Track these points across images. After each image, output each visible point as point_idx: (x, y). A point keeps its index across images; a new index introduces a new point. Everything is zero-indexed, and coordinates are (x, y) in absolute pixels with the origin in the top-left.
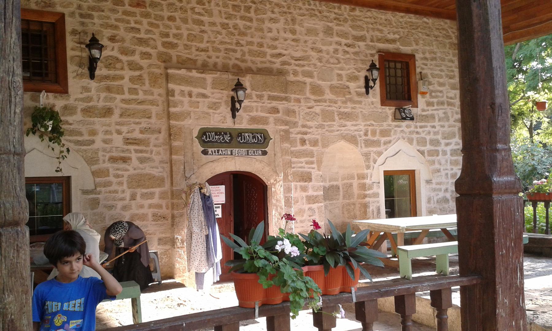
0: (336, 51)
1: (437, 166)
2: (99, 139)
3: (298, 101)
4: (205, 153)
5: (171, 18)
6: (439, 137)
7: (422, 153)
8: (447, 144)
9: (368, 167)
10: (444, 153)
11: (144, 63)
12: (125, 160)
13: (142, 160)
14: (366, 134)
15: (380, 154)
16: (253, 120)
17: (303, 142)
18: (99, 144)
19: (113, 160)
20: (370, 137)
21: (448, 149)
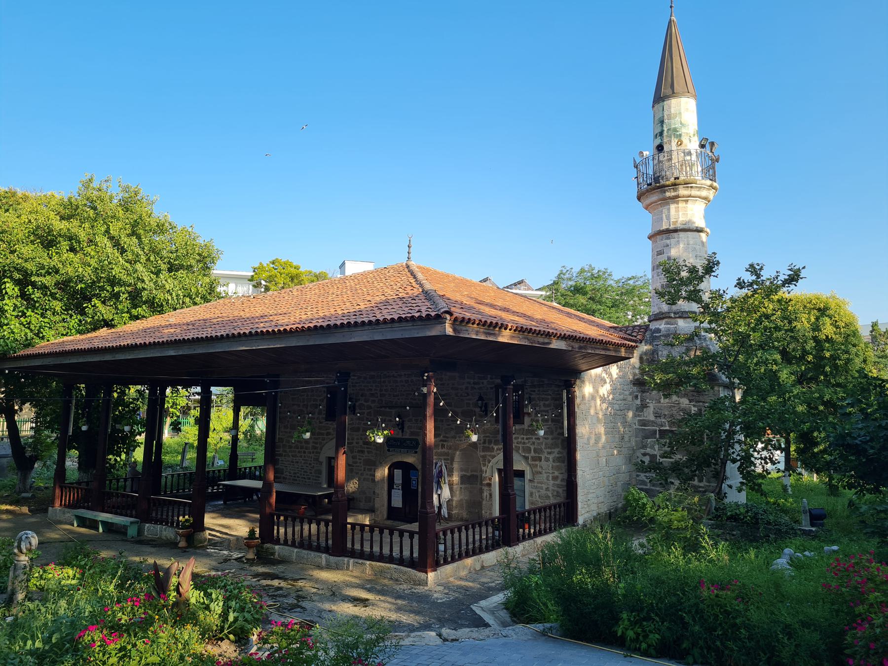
0: (467, 388)
1: (539, 469)
2: (355, 441)
3: (442, 421)
4: (389, 450)
5: (384, 382)
6: (532, 447)
7: (526, 458)
8: (550, 453)
9: (484, 465)
10: (547, 460)
11: (373, 405)
12: (362, 452)
13: (368, 452)
14: (484, 443)
15: (494, 457)
16: (412, 433)
18: (355, 444)
19: (359, 451)
20: (487, 445)
21: (551, 457)
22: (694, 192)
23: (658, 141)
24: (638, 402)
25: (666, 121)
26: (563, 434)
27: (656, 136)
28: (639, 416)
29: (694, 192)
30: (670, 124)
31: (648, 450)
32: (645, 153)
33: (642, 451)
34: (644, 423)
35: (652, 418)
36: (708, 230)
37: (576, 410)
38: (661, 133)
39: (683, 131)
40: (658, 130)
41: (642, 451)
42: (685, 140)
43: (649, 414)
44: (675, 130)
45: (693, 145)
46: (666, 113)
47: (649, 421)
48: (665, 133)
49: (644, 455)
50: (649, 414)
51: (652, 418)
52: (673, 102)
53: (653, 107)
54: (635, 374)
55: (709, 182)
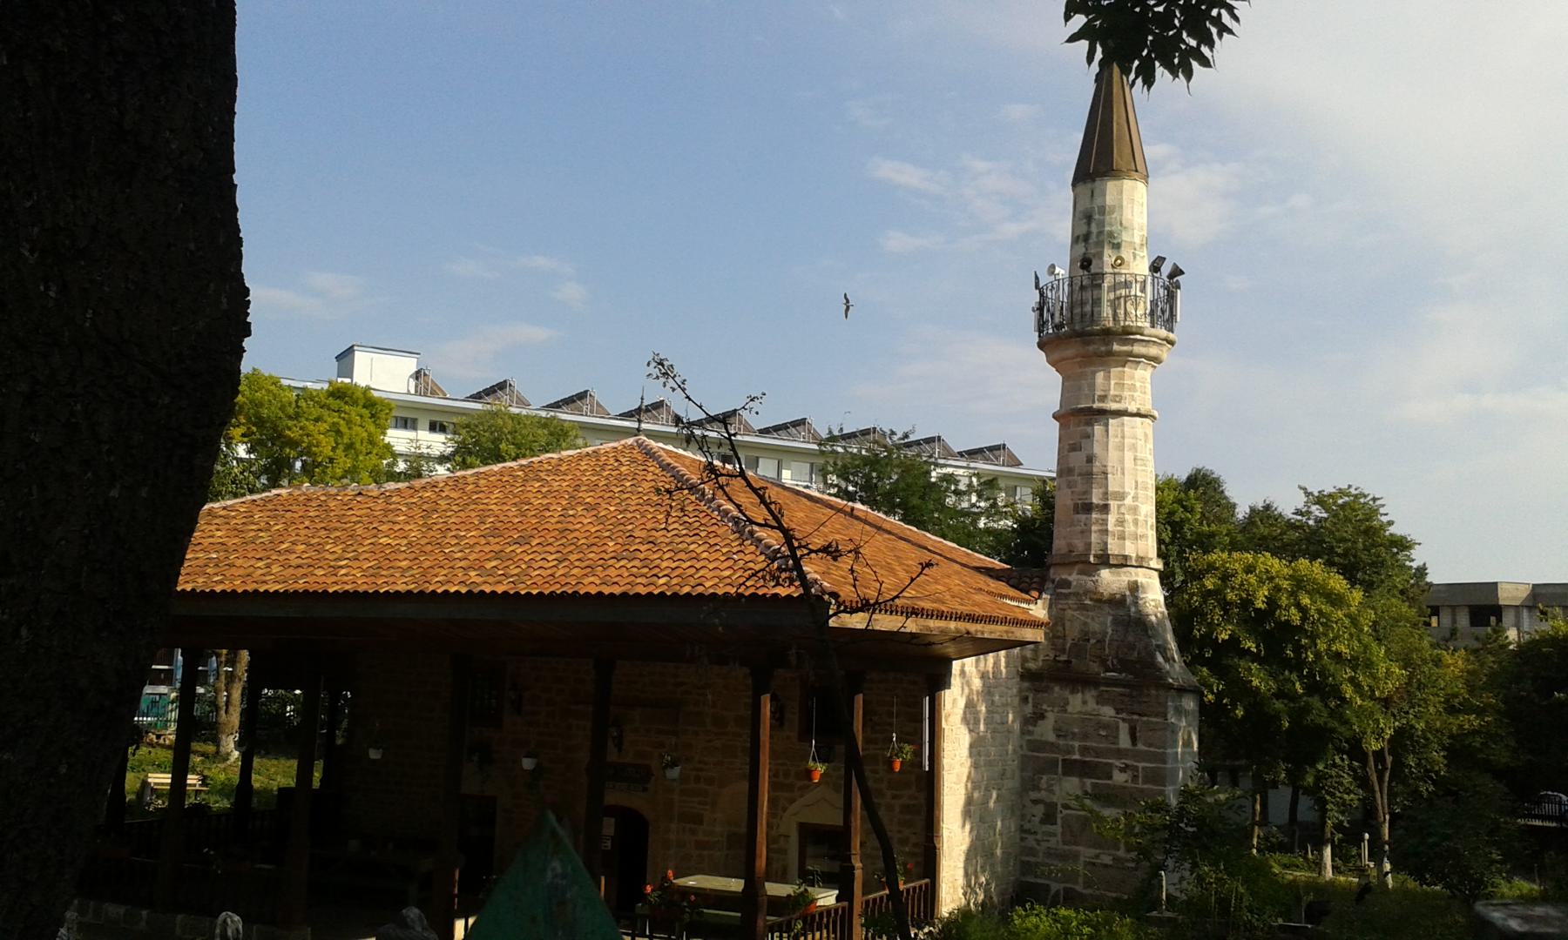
17: (697, 779)
22: (1137, 349)
23: (1081, 249)
24: (1029, 709)
25: (1097, 217)
26: (921, 765)
27: (1076, 240)
28: (1030, 733)
29: (1137, 349)
30: (1102, 224)
31: (1043, 795)
32: (1057, 270)
33: (1034, 795)
34: (1037, 746)
35: (1051, 737)
36: (1156, 413)
37: (944, 725)
38: (1086, 238)
39: (1125, 237)
40: (1083, 230)
41: (1034, 795)
42: (1126, 253)
43: (1046, 730)
44: (1111, 234)
45: (1141, 267)
46: (1098, 201)
47: (1046, 743)
48: (1093, 238)
49: (1035, 802)
50: (1046, 730)
51: (1051, 737)
52: (1111, 186)
53: (1074, 185)
54: (1024, 660)
55: (1163, 333)
